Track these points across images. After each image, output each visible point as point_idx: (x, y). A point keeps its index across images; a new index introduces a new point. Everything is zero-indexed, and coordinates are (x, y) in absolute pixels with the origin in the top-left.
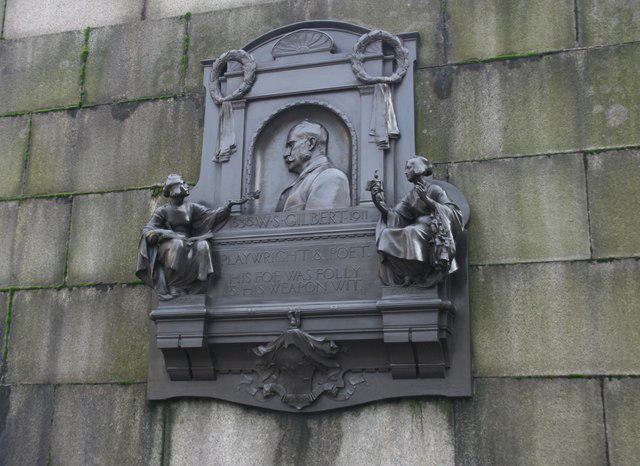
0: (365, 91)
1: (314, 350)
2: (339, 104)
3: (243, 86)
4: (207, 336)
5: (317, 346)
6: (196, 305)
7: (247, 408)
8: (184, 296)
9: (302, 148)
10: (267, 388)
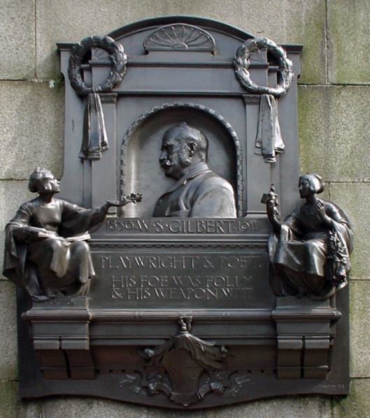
1: (203, 353)
2: (227, 113)
5: (208, 350)
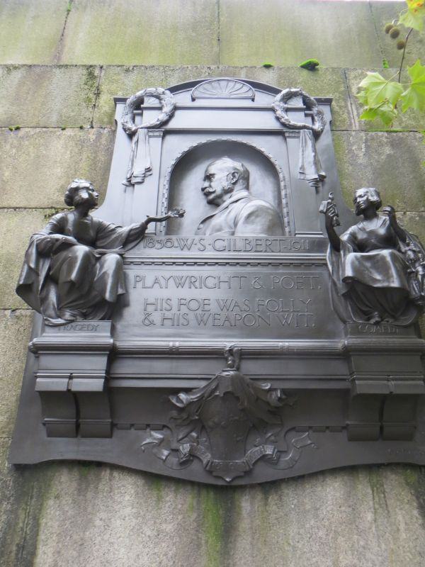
0: (291, 135)
3: (162, 116)
4: (109, 377)
6: (98, 333)
7: (154, 479)
8: (81, 322)
9: (217, 186)
10: (185, 448)
